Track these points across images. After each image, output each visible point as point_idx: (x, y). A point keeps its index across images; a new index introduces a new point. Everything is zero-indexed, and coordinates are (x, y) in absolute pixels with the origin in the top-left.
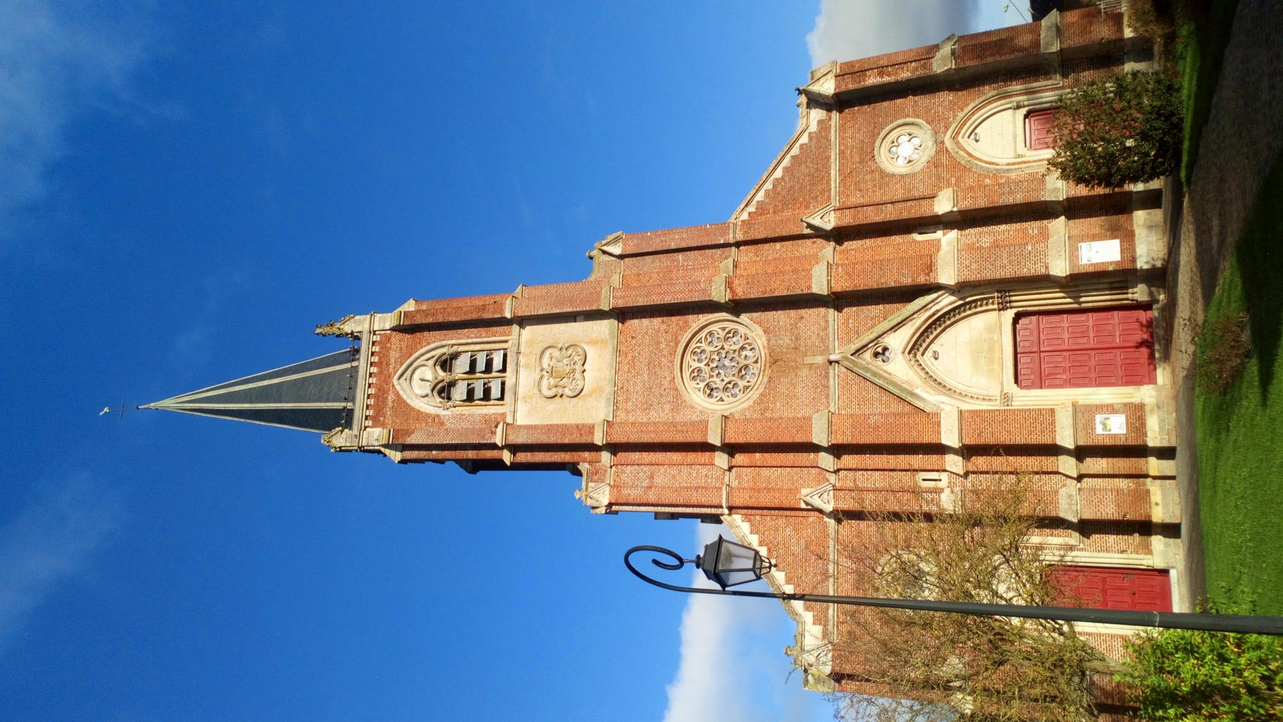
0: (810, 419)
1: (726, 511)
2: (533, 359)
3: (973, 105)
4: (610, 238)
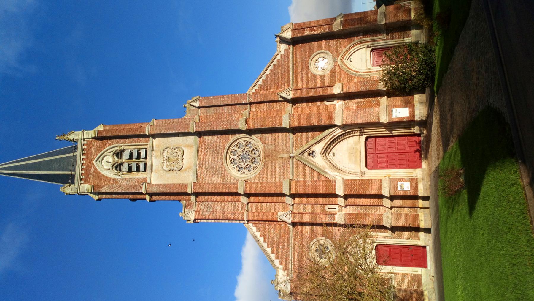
0: (282, 182)
1: (246, 222)
2: (159, 153)
3: (349, 45)
4: (194, 98)
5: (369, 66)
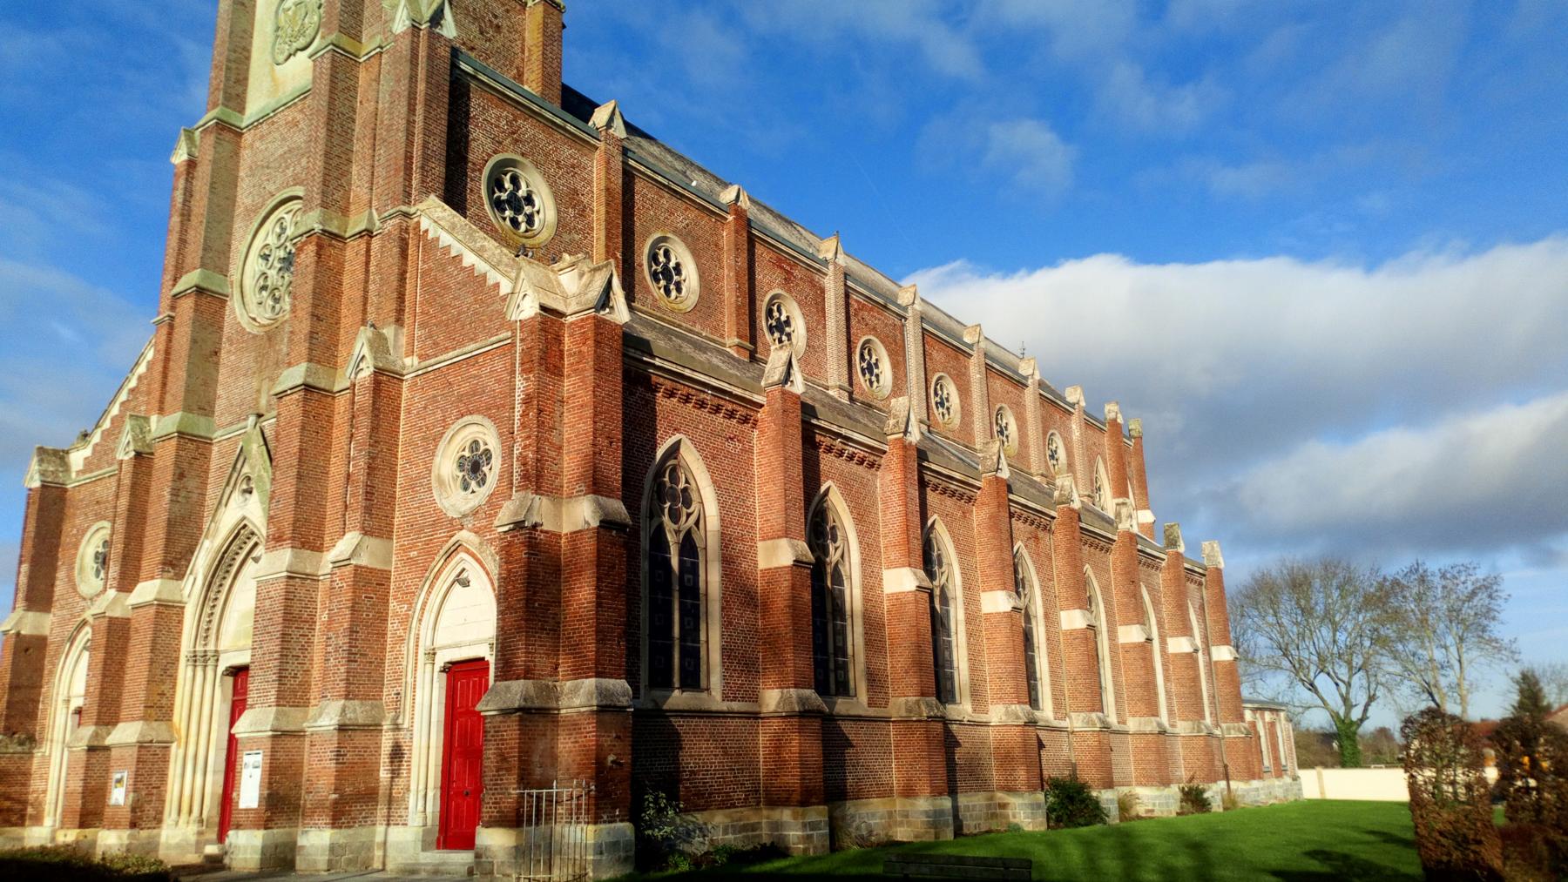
5: (443, 658)
